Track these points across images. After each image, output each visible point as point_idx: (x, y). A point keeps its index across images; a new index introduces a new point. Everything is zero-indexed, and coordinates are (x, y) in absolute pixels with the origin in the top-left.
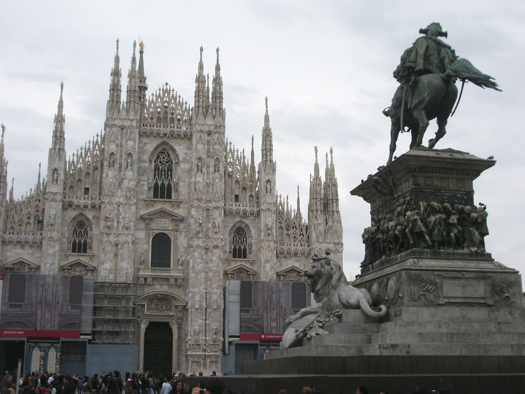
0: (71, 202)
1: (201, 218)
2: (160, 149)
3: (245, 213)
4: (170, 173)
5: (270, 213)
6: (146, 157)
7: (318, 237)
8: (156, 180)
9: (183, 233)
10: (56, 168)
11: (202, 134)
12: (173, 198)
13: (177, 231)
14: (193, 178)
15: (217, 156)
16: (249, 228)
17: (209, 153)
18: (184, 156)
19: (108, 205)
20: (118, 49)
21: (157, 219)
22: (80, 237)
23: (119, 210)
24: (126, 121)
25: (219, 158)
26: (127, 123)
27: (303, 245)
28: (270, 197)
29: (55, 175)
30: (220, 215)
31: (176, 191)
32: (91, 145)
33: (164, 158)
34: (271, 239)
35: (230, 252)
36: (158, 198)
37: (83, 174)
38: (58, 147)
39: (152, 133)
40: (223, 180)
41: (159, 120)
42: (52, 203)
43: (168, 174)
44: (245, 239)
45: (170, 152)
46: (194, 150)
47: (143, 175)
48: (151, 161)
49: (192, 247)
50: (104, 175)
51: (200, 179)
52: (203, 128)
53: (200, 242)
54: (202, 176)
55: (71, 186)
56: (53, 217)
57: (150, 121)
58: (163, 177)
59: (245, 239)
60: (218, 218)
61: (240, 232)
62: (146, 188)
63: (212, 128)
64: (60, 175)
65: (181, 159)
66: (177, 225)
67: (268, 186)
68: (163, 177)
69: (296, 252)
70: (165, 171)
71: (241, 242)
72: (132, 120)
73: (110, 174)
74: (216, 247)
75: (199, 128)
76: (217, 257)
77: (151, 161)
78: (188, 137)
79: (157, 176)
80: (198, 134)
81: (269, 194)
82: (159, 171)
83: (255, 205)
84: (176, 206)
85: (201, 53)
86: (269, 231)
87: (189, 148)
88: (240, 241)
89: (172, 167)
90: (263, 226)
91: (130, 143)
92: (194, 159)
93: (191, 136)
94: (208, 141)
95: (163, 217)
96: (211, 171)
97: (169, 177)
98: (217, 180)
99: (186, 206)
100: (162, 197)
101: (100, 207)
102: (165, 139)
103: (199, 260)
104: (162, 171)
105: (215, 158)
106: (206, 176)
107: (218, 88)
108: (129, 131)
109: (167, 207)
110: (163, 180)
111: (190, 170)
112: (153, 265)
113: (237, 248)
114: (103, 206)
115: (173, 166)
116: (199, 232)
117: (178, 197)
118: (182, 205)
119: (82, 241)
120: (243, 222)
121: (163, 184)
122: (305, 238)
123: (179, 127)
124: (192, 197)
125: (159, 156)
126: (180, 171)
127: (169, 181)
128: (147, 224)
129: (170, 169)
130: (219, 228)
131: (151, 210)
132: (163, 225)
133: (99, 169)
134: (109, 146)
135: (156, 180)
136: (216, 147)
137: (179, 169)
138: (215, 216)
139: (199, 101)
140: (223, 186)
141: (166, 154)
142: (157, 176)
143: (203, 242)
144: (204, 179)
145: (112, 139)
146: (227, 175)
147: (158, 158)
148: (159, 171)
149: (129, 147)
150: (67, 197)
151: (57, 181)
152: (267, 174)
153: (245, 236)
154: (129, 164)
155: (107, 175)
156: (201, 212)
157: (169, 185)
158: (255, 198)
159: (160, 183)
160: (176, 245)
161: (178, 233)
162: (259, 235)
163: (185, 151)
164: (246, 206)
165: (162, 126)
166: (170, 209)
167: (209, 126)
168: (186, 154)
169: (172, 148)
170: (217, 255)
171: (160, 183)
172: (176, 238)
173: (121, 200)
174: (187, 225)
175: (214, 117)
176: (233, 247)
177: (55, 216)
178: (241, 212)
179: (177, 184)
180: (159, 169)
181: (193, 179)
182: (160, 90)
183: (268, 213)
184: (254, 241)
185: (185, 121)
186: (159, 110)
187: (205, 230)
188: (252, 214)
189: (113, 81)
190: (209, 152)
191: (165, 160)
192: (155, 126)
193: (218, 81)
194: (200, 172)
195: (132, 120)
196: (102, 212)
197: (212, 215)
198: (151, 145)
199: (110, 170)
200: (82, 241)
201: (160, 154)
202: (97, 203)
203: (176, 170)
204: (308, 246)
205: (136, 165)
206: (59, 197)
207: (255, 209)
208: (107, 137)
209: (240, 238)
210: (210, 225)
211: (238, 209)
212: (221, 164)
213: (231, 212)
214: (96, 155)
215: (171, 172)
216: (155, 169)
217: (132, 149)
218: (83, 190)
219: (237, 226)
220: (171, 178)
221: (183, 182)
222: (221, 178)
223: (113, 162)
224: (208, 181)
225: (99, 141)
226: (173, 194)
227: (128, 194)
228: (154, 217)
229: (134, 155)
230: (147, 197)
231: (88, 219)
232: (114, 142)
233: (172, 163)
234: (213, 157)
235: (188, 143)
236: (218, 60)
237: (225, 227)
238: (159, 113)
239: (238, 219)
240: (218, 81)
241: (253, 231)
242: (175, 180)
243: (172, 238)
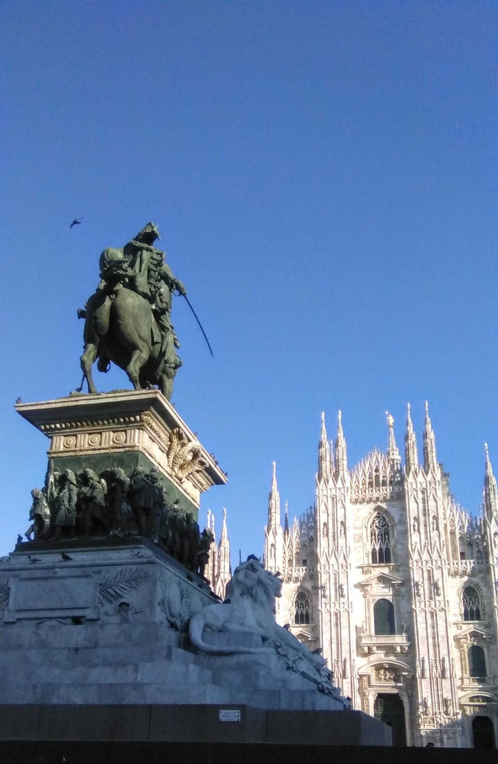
4: (387, 537)
8: (374, 545)
18: (400, 517)
22: (302, 609)
32: (306, 518)
36: (377, 563)
39: (363, 500)
41: (371, 484)
43: (385, 538)
44: (476, 600)
45: (385, 516)
59: (476, 600)
61: (470, 592)
70: (381, 535)
71: (473, 603)
82: (375, 536)
88: (471, 602)
97: (387, 541)
100: (381, 561)
112: (377, 632)
118: (402, 568)
119: (304, 613)
135: (374, 545)
142: (374, 541)
147: (373, 523)
148: (375, 536)
157: (387, 549)
158: (483, 554)
160: (399, 611)
163: (400, 512)
165: (374, 490)
179: (395, 546)
200: (304, 613)
203: (393, 532)
209: (470, 599)
215: (388, 536)
216: (372, 535)
221: (401, 544)
225: (313, 513)
231: (308, 591)
233: (388, 526)
242: (392, 543)
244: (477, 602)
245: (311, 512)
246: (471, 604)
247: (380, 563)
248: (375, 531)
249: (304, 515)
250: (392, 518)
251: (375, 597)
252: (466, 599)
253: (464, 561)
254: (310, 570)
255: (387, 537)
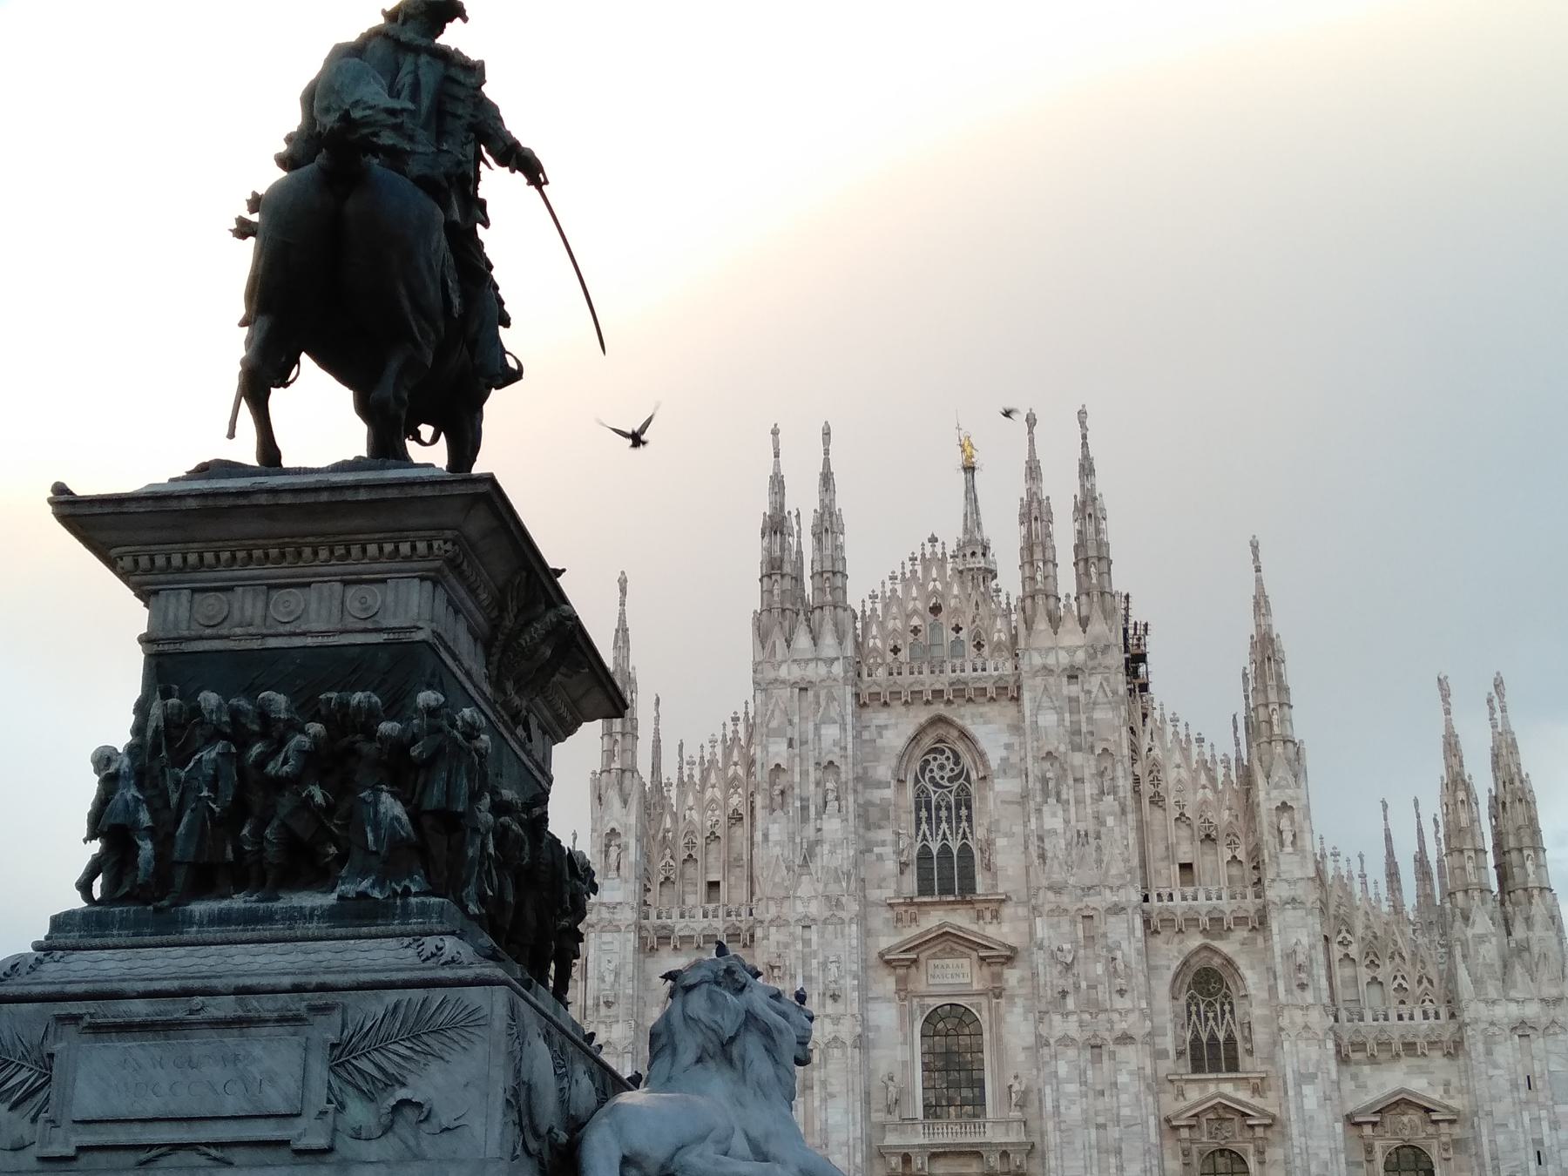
0: (664, 928)
1: (1067, 946)
2: (928, 741)
3: (1217, 921)
4: (964, 812)
5: (1301, 913)
6: (883, 771)
7: (1477, 982)
8: (924, 838)
9: (1019, 1001)
10: (613, 830)
11: (1051, 680)
12: (980, 889)
13: (998, 996)
14: (1033, 820)
15: (1104, 745)
16: (1236, 970)
17: (1077, 739)
18: (1004, 753)
19: (773, 930)
20: (777, 455)
21: (932, 962)
23: (807, 943)
24: (812, 665)
25: (1112, 749)
26: (815, 672)
27: (1431, 1014)
28: (1297, 858)
29: (613, 851)
30: (1132, 931)
31: (988, 867)
32: (719, 750)
33: (942, 767)
34: (1310, 1000)
35: (1180, 1054)
36: (933, 894)
37: (700, 841)
38: (616, 765)
40: (1131, 818)
42: (607, 937)
43: (959, 817)
44: (1227, 1007)
45: (960, 747)
46: (1028, 731)
47: (880, 827)
48: (901, 782)
49: (1048, 1044)
50: (758, 837)
51: (1053, 820)
52: (1051, 661)
53: (1071, 1027)
54: (1060, 813)
55: (667, 878)
56: (610, 978)
57: (890, 656)
58: (944, 825)
59: (1227, 1007)
60: (1124, 945)
61: (1208, 983)
62: (891, 866)
63: (1080, 656)
64: (626, 848)
65: (994, 763)
66: (997, 977)
67: (1285, 823)
68: (944, 825)
69: (1410, 1039)
70: (949, 808)
71: (1215, 1019)
72: (832, 661)
73: (776, 831)
74: (1125, 1039)
75: (1037, 660)
76: (1131, 1073)
77: (901, 782)
78: (1009, 692)
79: (924, 826)
80: (1038, 680)
81: (1289, 849)
82: (929, 810)
83: (1250, 892)
84: (988, 915)
85: (1031, 432)
86: (1303, 975)
87: (1017, 729)
88: (1211, 1015)
89: (969, 794)
90: (1278, 960)
91: (831, 732)
92: (1029, 760)
93: (1019, 688)
94: (1070, 699)
95: (952, 953)
96: (1088, 792)
98: (1110, 821)
99: (1022, 911)
101: (752, 936)
102: (940, 709)
103: (1072, 1088)
104: (938, 808)
105: (1098, 751)
106: (1073, 810)
107: (1091, 529)
108: (823, 693)
109: (961, 919)
110: (944, 837)
111: (1025, 797)
113: (1204, 1037)
114: (759, 933)
115: (972, 789)
116: (1064, 994)
117: (995, 886)
118: (1007, 911)
120: (1216, 952)
121: (945, 850)
122: (1438, 990)
123: (979, 666)
124: (1033, 884)
125: (927, 762)
126: (996, 800)
127: (964, 837)
128: (902, 982)
129: (964, 801)
130: (1129, 977)
131: (911, 932)
132: (954, 976)
133: (747, 820)
134: (765, 748)
135: (924, 838)
136: (1098, 715)
137: (991, 795)
138: (1113, 937)
139: (1033, 578)
140: (1132, 837)
141: (948, 753)
142: (924, 826)
143: (1081, 1024)
144: (1067, 822)
145: (774, 724)
146: (1146, 801)
148: (929, 810)
149: (827, 742)
150: (653, 914)
151: (618, 868)
152: (1277, 786)
153: (1226, 996)
154: (831, 796)
155: (766, 836)
156: (1066, 927)
157: (965, 850)
158: (1248, 866)
159: (935, 847)
161: (1002, 1001)
162: (1272, 990)
163: (1005, 738)
164: (1219, 898)
165: (926, 670)
166: (974, 928)
167: (1071, 651)
168: (1008, 747)
169: (964, 735)
170: (1133, 1067)
171: (935, 847)
172: (998, 1020)
173: (814, 909)
174: (1028, 974)
175: (1084, 622)
176: (1189, 1036)
177: (617, 975)
178: (1204, 920)
179: (990, 843)
180: (928, 803)
181: (1033, 825)
182: (913, 559)
183: (1290, 914)
184: (1257, 1012)
185: (998, 647)
186: (916, 621)
187: (1084, 985)
188: (1240, 921)
189: (769, 550)
190: (1079, 732)
191: (947, 774)
192: (905, 670)
193: (1088, 508)
194: (1052, 800)
195: (832, 661)
196: (758, 952)
197: (1105, 935)
198: (896, 730)
199: (775, 822)
201: (930, 757)
202: (744, 926)
203: (983, 799)
204: (1452, 1016)
205: (851, 798)
206: (628, 916)
207: (1250, 904)
208: (758, 720)
209: (1210, 1004)
210: (1100, 969)
211: (1190, 908)
212: (1119, 768)
213: (1168, 922)
214: (735, 777)
215: (969, 808)
217: (837, 749)
218: (702, 888)
219: (1196, 964)
220: (970, 826)
221: (1006, 835)
222: (1124, 812)
223: (782, 793)
224: (1082, 827)
225: (742, 735)
226: (979, 878)
227: (834, 889)
228: (923, 957)
229: (843, 768)
230: (898, 893)
232: (778, 732)
233: (968, 779)
234: (1092, 748)
235: (1011, 709)
236: (1085, 445)
237: (1151, 970)
238: (916, 631)
239: (1195, 941)
240: (1089, 510)
241: (1252, 978)
242: (980, 833)
243: (984, 1018)
244: (1228, 1016)
245: (736, 732)
246: (1211, 1022)
247: (941, 893)
248: (928, 796)
249: (713, 742)
250: (982, 755)
251: (929, 1001)
252: (1197, 1005)
253: (1189, 890)
254: (729, 915)
255: (964, 812)
